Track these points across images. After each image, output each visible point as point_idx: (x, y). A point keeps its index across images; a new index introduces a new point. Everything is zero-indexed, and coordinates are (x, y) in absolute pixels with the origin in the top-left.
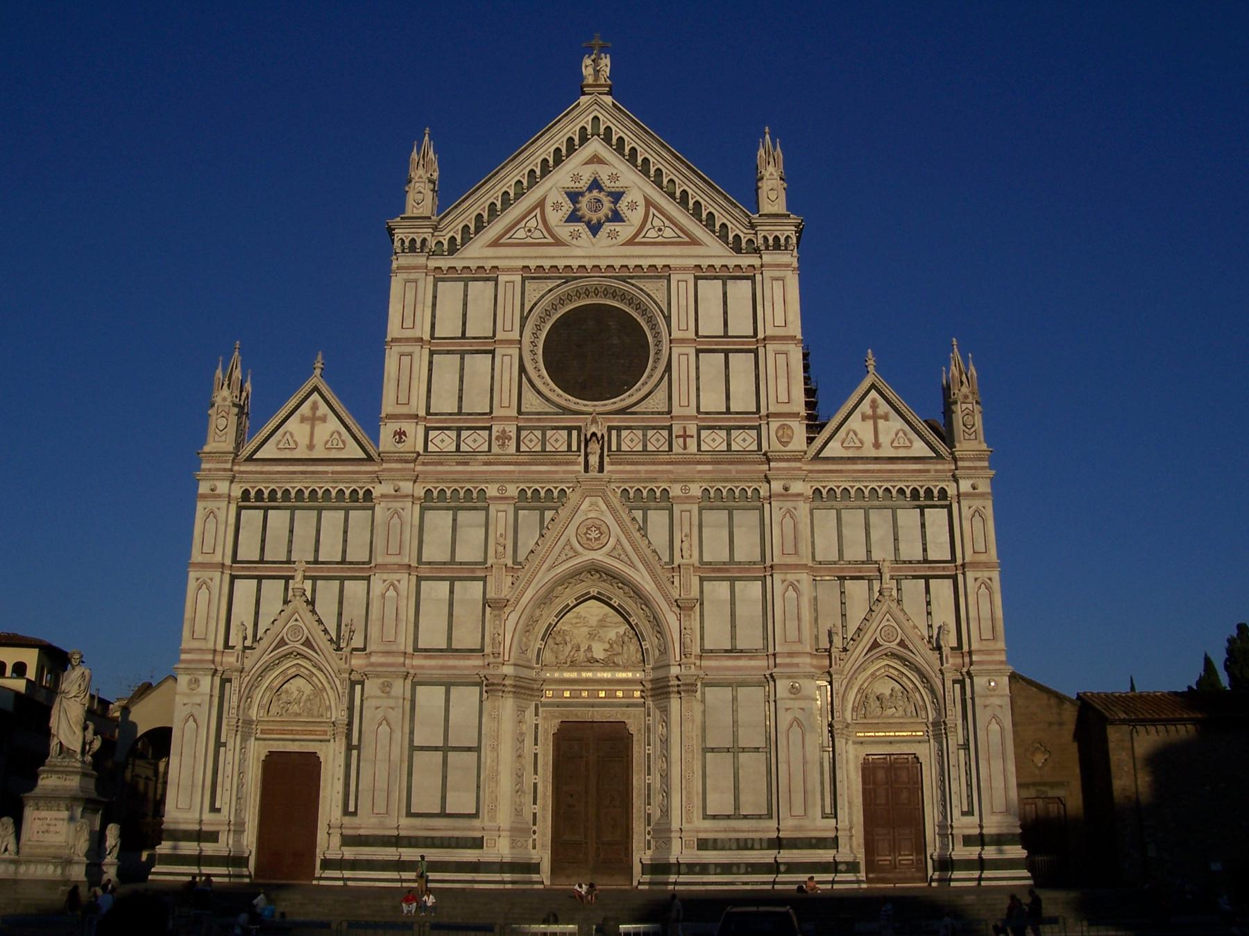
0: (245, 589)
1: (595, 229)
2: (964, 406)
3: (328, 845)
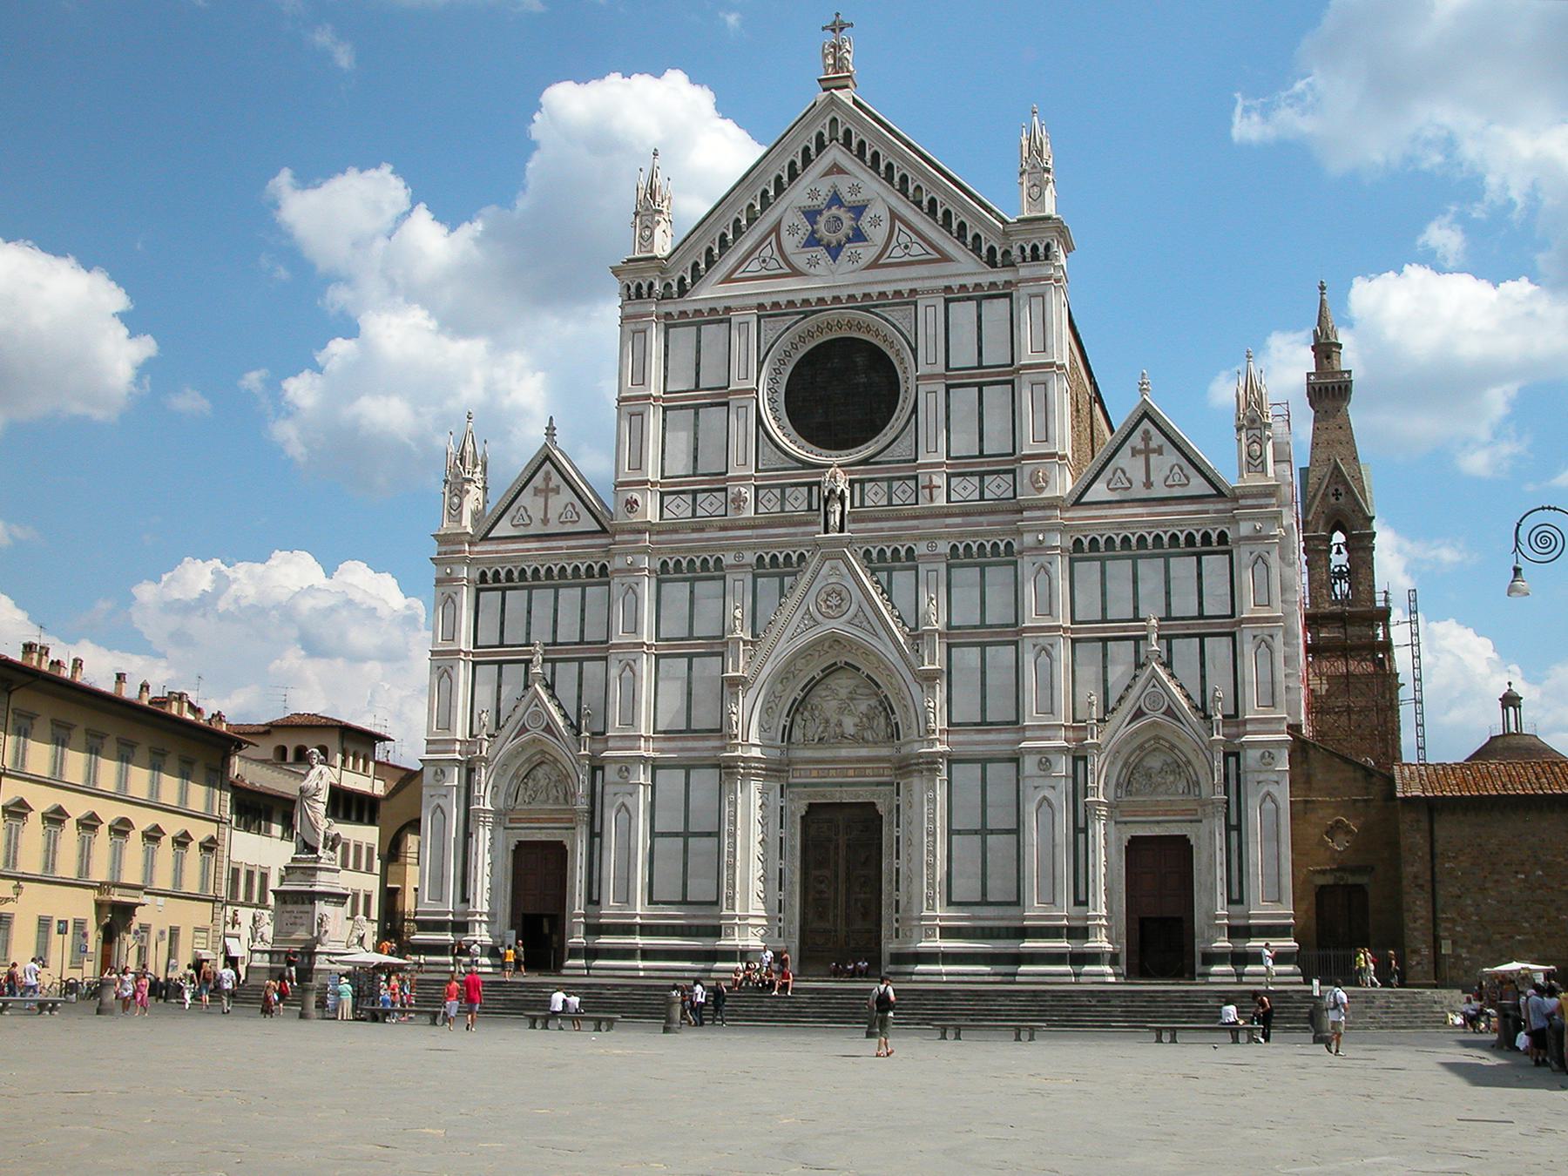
1: (834, 251)
2: (1251, 433)
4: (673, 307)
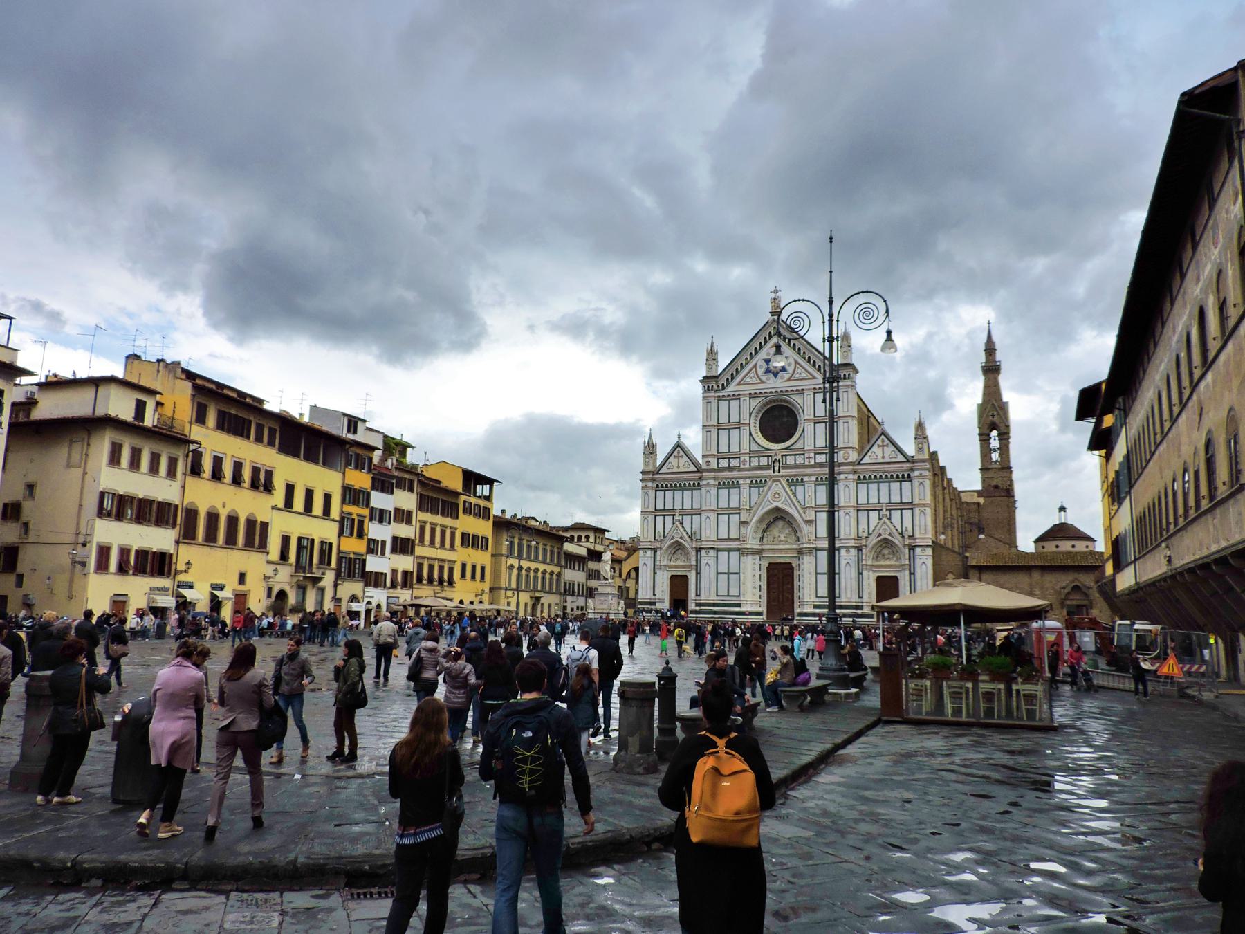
1: (775, 375)
3: (692, 606)
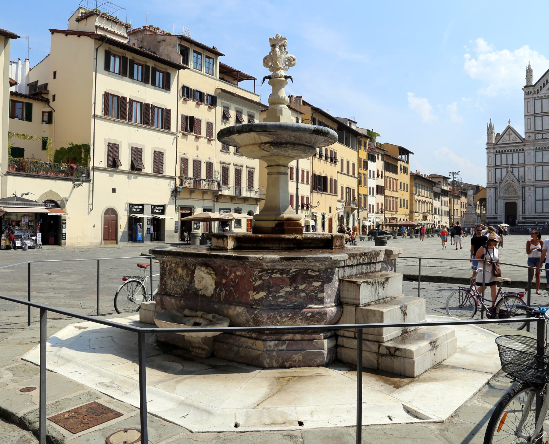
0: (498, 171)
4: (536, 96)
